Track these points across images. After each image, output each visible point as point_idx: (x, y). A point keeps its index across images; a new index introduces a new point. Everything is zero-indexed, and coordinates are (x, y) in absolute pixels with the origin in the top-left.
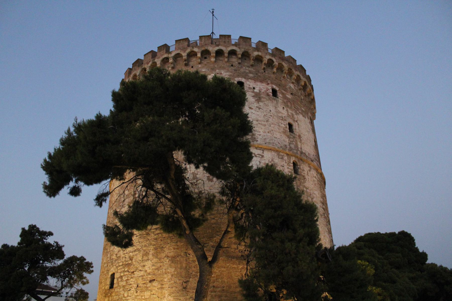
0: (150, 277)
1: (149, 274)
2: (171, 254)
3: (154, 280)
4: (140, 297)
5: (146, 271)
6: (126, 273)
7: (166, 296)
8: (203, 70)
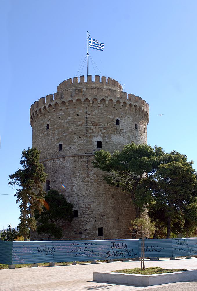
0: (102, 214)
1: (101, 213)
2: (112, 205)
3: (104, 216)
4: (98, 222)
5: (100, 212)
6: (86, 211)
7: (110, 222)
8: (122, 114)
